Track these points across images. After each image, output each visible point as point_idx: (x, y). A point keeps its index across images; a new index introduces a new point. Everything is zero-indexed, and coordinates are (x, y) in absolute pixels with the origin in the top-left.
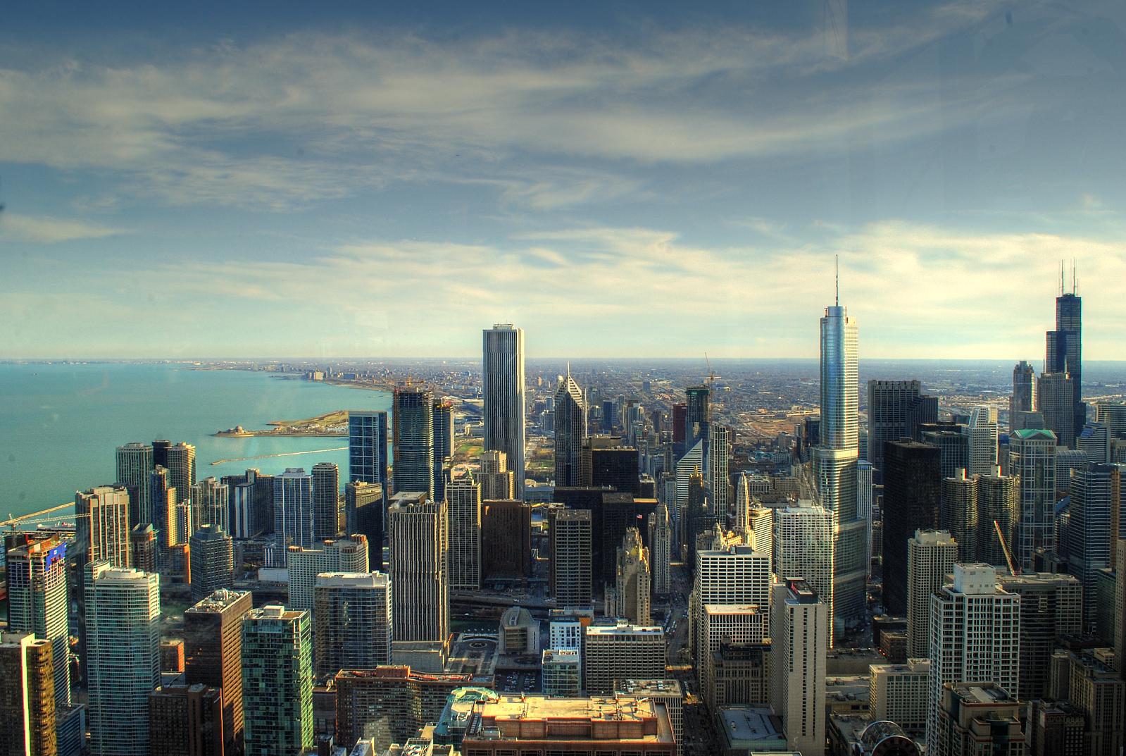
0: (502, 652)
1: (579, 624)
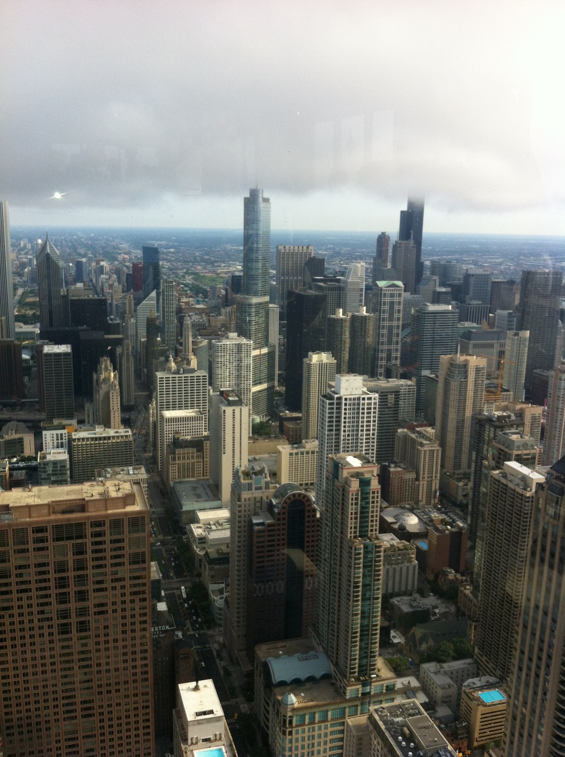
1: (65, 431)
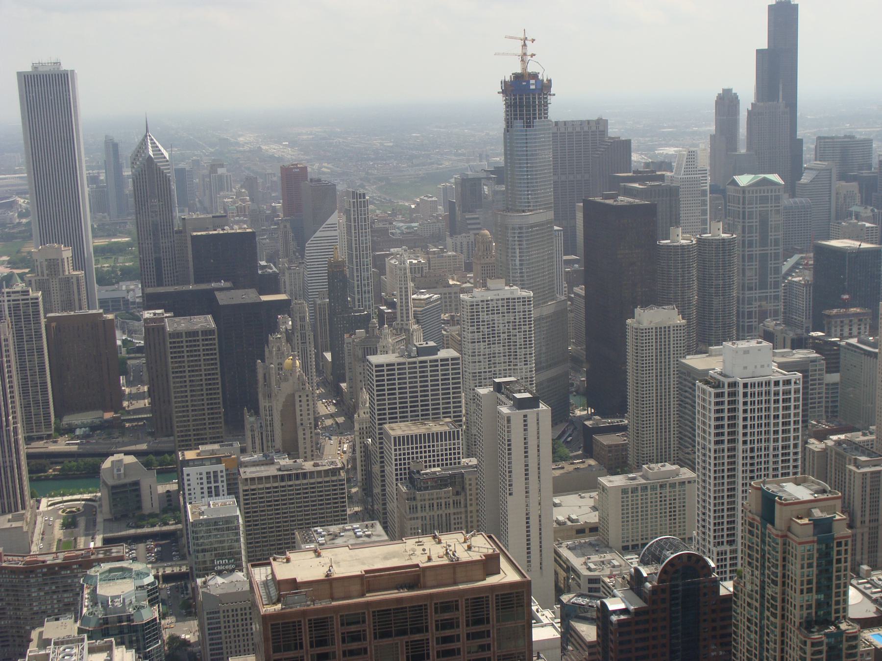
0: (109, 516)
1: (222, 467)
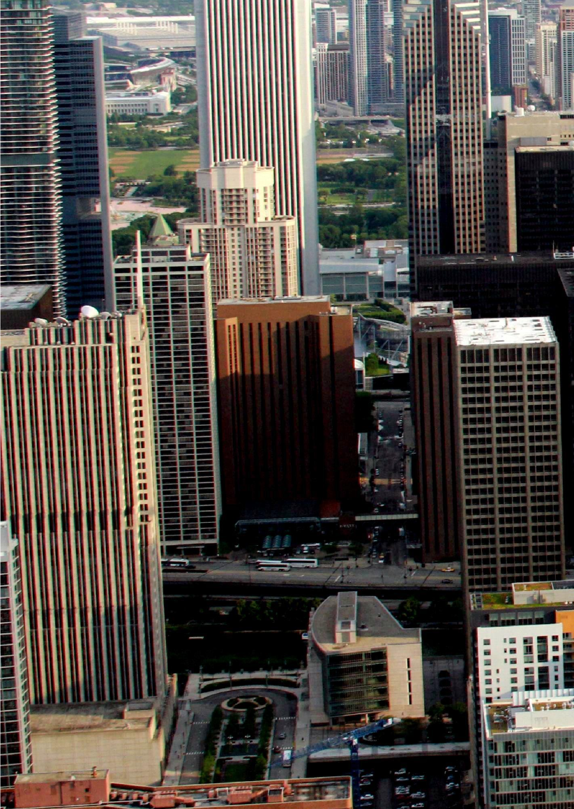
0: (321, 718)
